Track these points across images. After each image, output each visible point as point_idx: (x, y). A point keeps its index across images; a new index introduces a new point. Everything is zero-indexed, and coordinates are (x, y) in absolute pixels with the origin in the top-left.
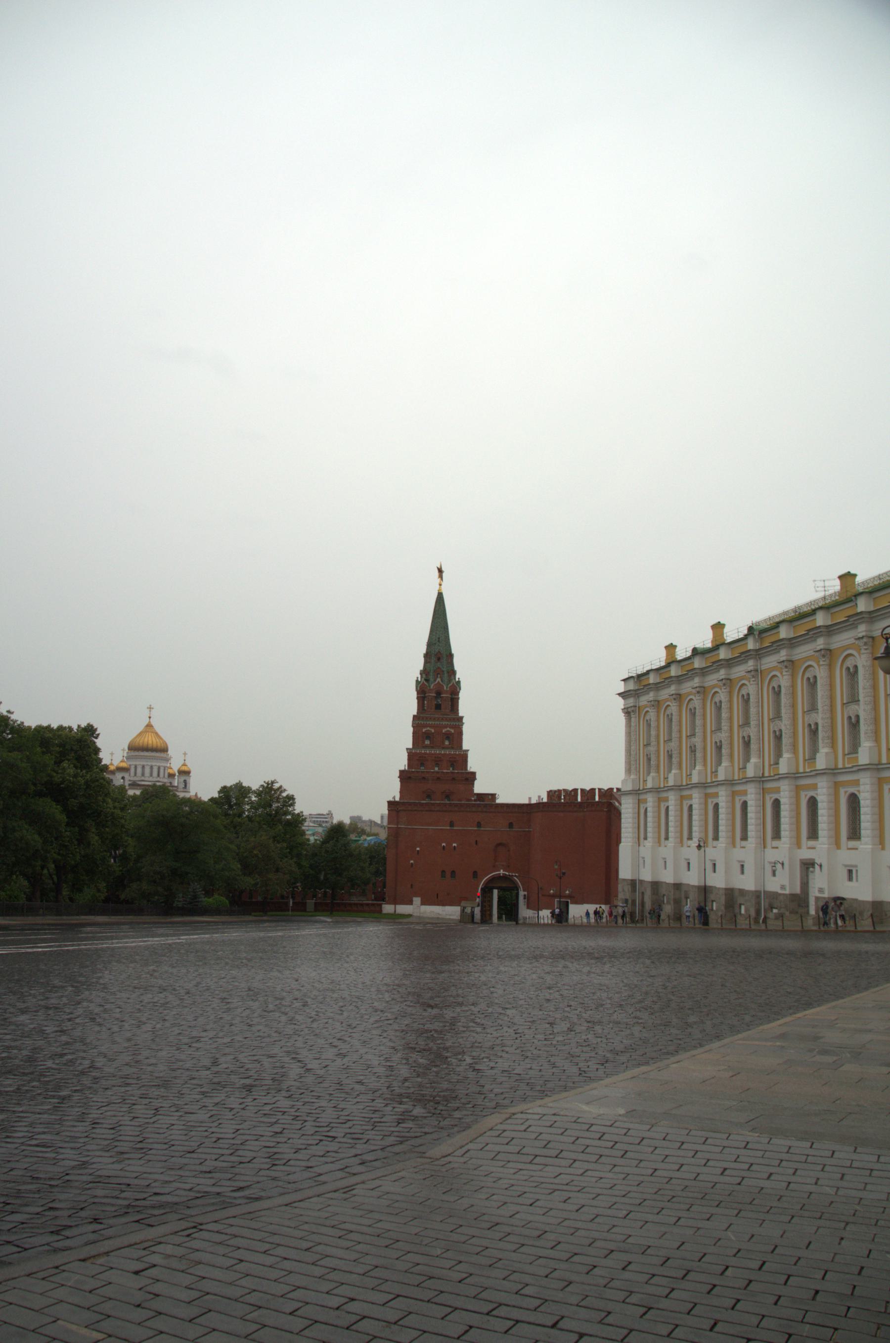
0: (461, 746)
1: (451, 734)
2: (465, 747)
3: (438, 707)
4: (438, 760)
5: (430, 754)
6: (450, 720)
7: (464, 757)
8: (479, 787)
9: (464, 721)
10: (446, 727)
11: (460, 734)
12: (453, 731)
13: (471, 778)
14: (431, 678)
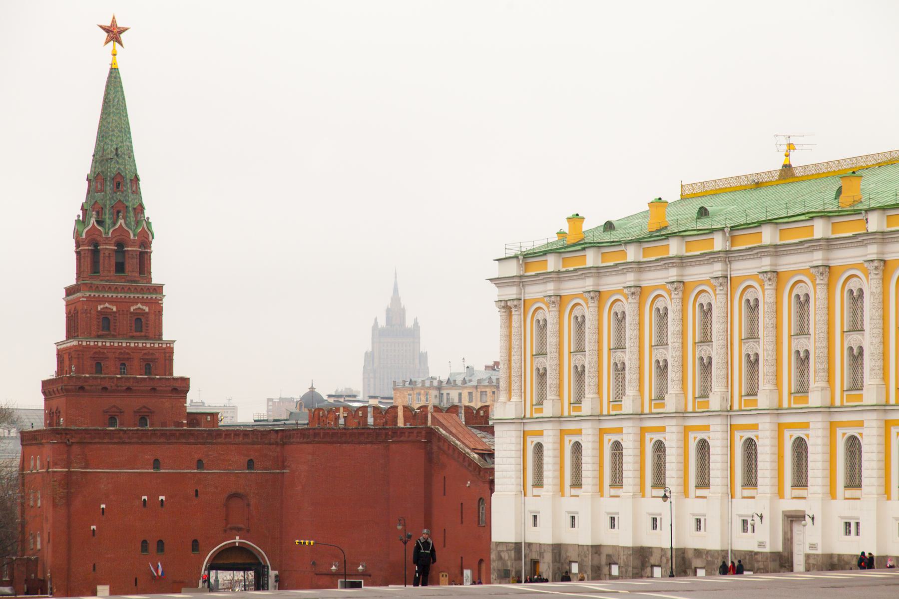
0: (160, 335)
1: (145, 314)
2: (165, 337)
3: (120, 267)
4: (124, 359)
5: (112, 347)
6: (142, 290)
7: (167, 354)
9: (165, 291)
10: (135, 302)
11: (158, 313)
12: (147, 310)
13: (182, 386)
14: (108, 222)
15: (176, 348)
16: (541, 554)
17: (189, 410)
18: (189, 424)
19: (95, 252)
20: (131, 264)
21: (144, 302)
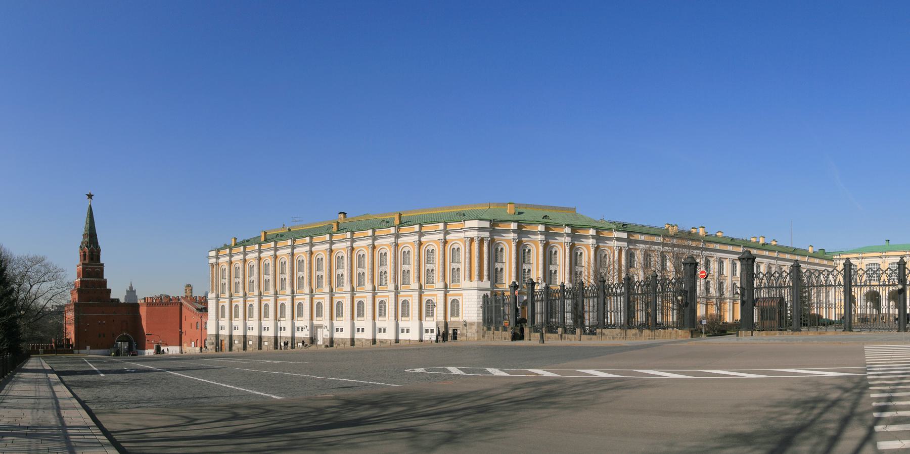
0: (102, 277)
4: (93, 283)
8: (113, 296)
19: (85, 255)
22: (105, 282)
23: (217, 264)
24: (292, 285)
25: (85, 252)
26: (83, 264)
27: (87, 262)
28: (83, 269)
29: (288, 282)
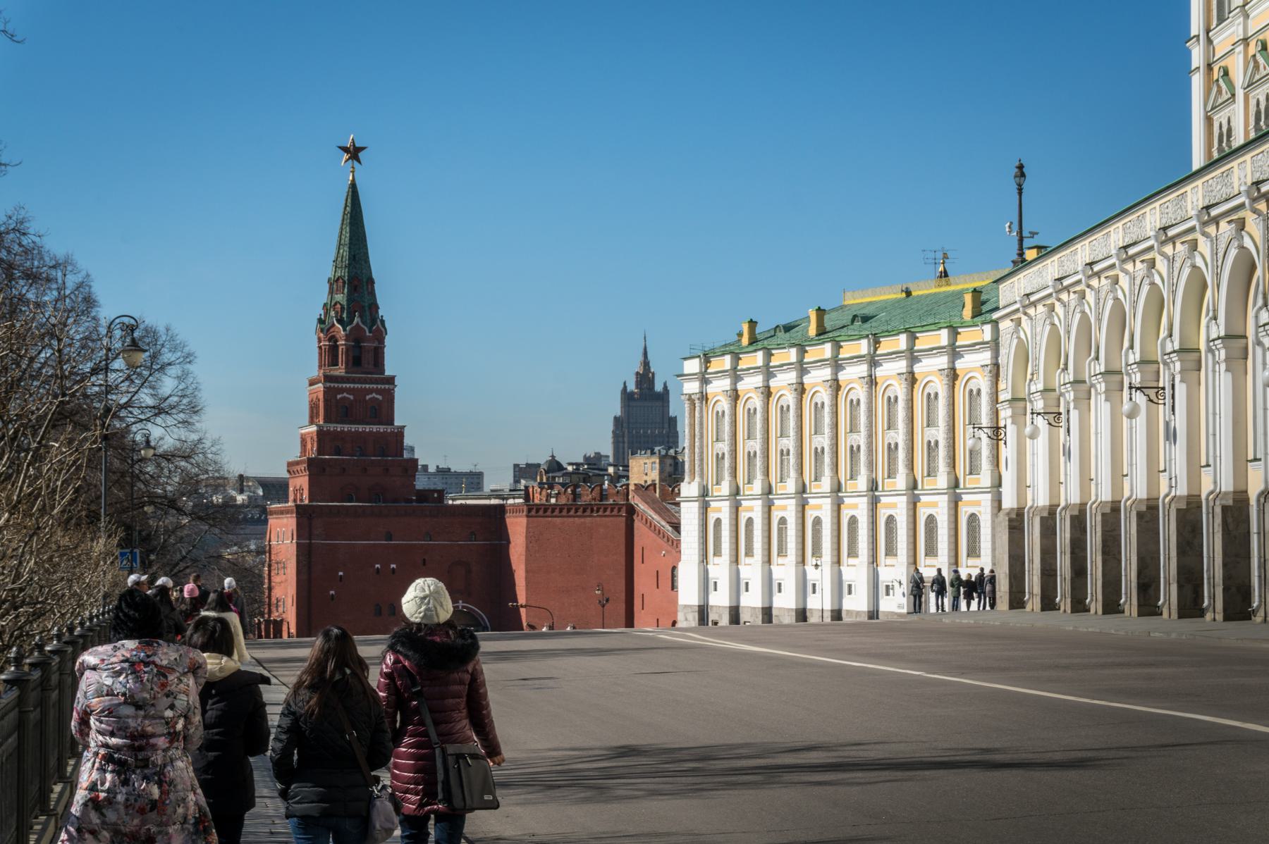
0: (390, 421)
2: (397, 423)
12: (380, 397)
15: (406, 432)
16: (720, 616)
17: (418, 487)
18: (418, 501)
19: (333, 349)
20: (367, 358)
21: (378, 391)
22: (399, 434)
23: (704, 397)
24: (952, 463)
25: (333, 339)
26: (328, 378)
27: (340, 370)
28: (327, 391)
29: (901, 455)
